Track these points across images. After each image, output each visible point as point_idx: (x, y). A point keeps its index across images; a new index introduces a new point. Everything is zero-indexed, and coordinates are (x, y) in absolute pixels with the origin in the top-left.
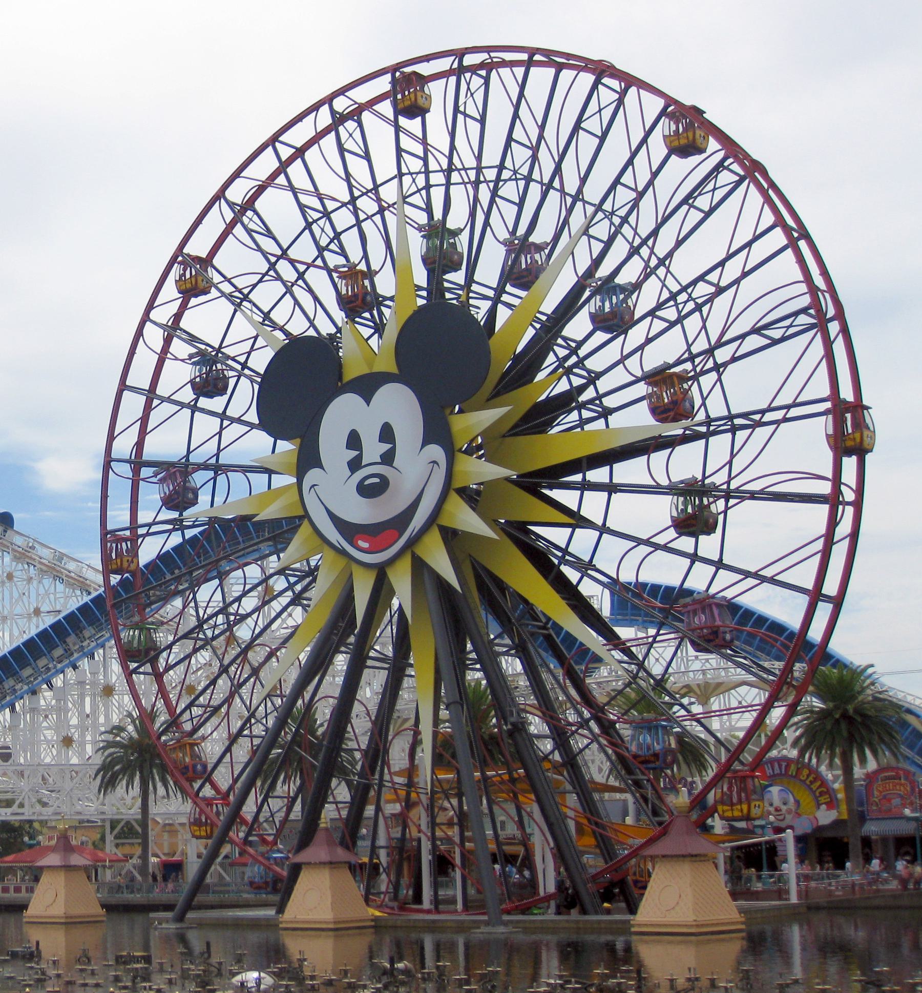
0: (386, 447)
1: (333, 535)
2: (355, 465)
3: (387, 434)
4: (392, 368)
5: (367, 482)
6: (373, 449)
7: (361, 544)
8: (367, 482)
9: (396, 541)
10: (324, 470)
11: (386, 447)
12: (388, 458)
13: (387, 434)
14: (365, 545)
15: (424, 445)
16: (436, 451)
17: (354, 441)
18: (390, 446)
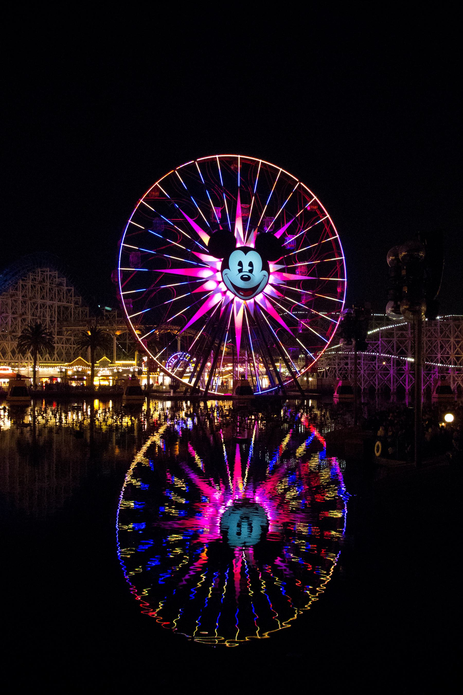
0: (251, 268)
1: (233, 289)
2: (240, 271)
3: (251, 264)
4: (252, 246)
5: (244, 277)
6: (246, 268)
7: (241, 293)
8: (244, 277)
9: (252, 295)
10: (229, 269)
11: (251, 268)
12: (251, 271)
13: (251, 264)
14: (242, 294)
15: (262, 270)
16: (265, 272)
18: (251, 268)
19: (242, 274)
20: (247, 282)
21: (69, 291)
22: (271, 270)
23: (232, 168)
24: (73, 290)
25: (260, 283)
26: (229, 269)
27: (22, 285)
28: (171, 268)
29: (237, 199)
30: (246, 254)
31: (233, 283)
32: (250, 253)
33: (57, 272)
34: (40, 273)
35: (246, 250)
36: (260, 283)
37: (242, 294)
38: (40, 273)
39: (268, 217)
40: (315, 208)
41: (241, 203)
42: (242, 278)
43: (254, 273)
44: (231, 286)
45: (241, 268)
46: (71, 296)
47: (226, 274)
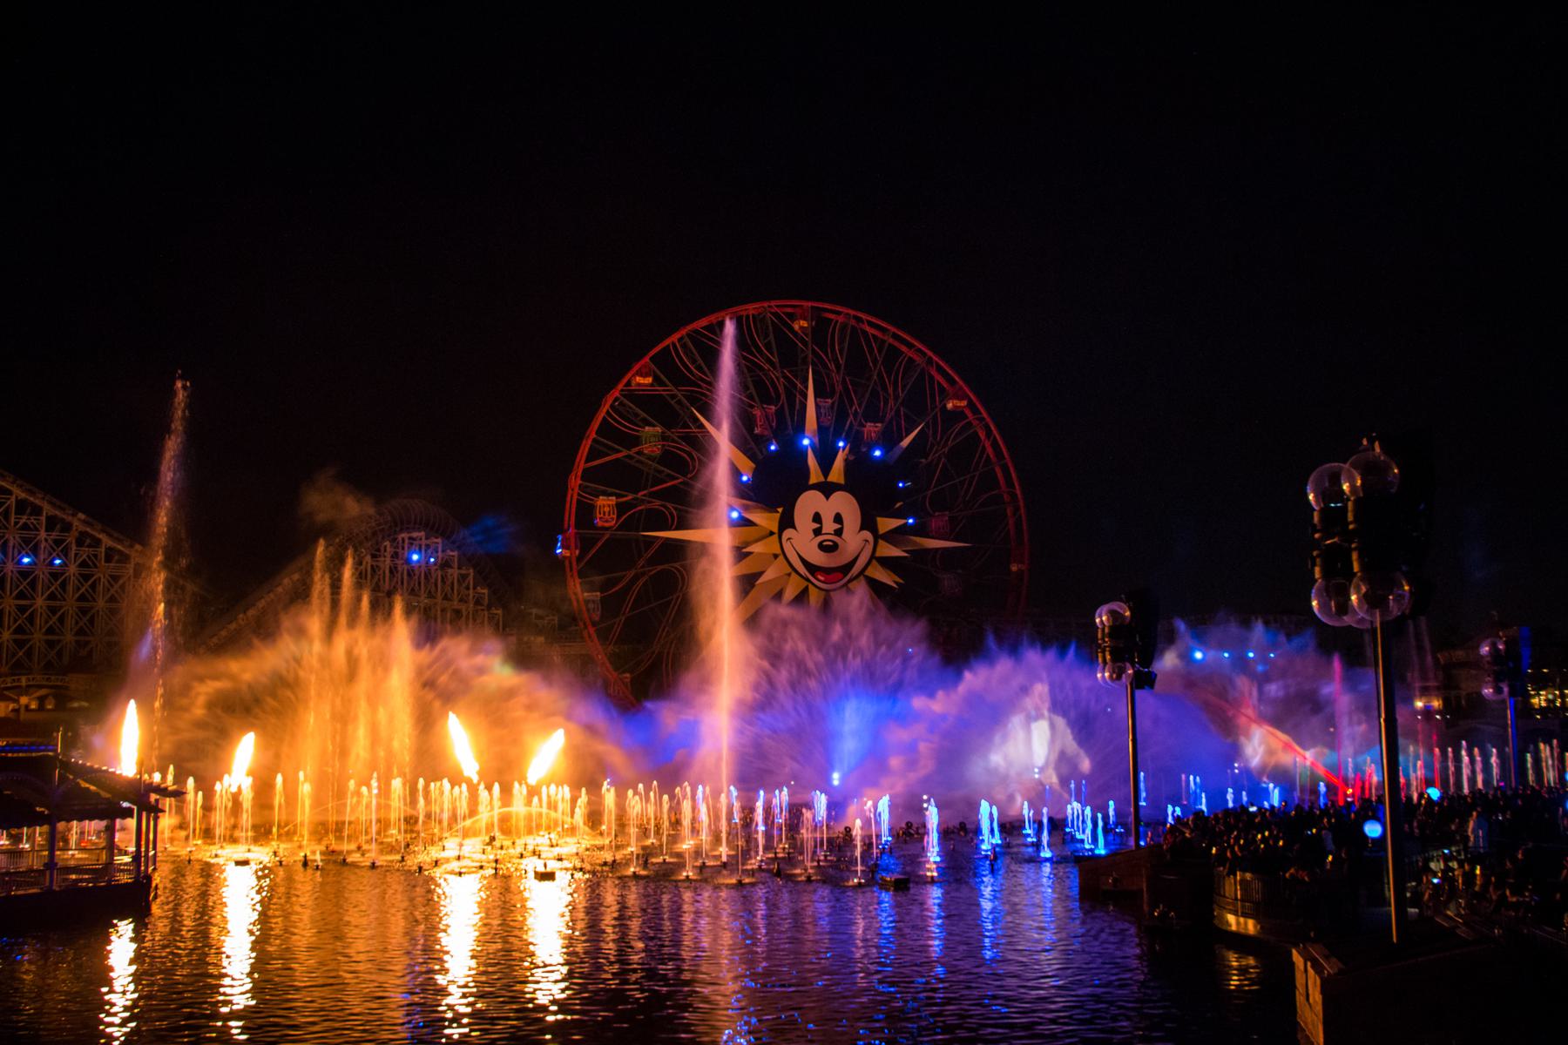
0: (840, 526)
2: (817, 532)
3: (838, 519)
4: (842, 481)
5: (825, 543)
6: (829, 526)
8: (825, 543)
12: (839, 532)
13: (838, 519)
14: (822, 578)
15: (862, 529)
16: (867, 535)
17: (817, 518)
19: (820, 538)
20: (832, 554)
21: (464, 577)
22: (882, 529)
23: (796, 327)
24: (471, 577)
26: (795, 528)
27: (372, 566)
28: (676, 529)
29: (807, 388)
30: (827, 499)
31: (806, 558)
33: (439, 540)
34: (407, 541)
35: (827, 489)
37: (822, 578)
38: (407, 541)
39: (869, 424)
41: (816, 397)
42: (821, 546)
43: (844, 536)
44: (801, 563)
45: (819, 525)
46: (468, 588)
47: (789, 539)
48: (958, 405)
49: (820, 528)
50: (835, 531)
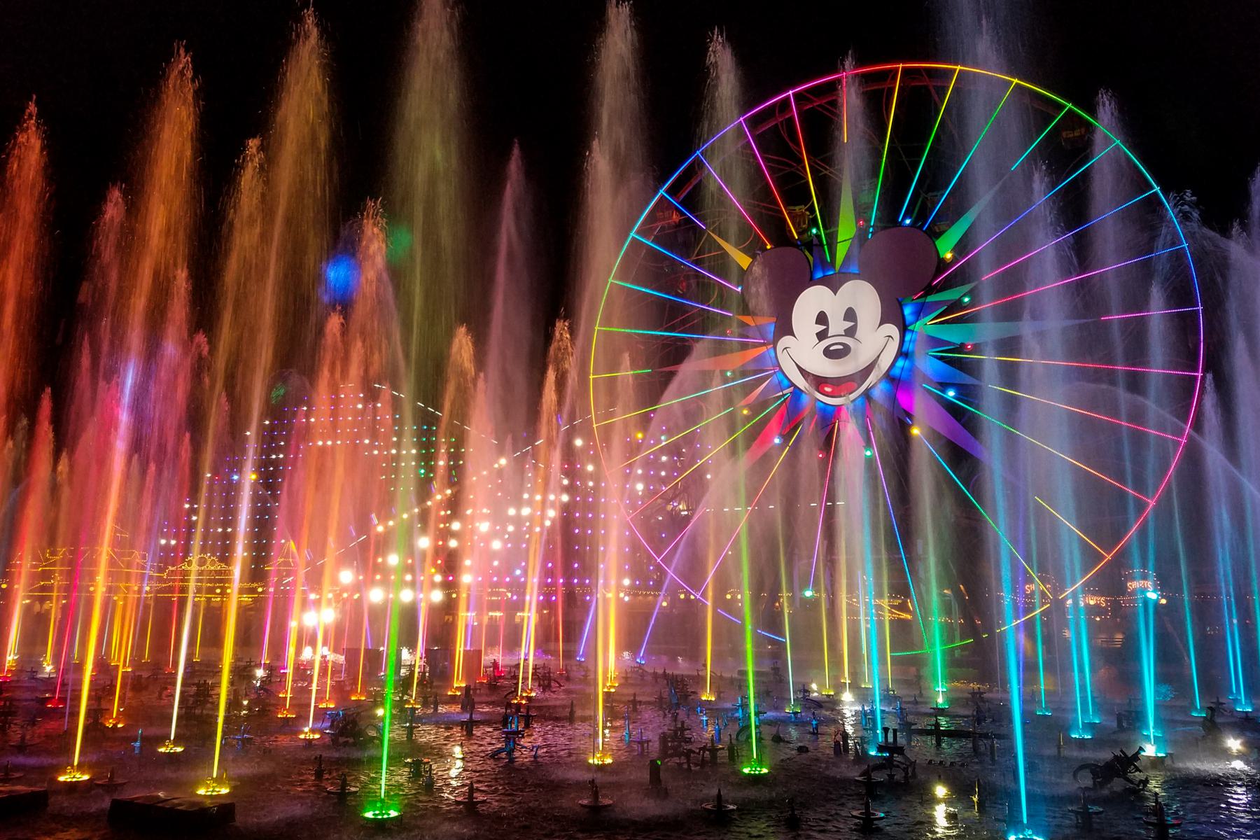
2: (822, 336)
3: (850, 315)
6: (837, 325)
8: (832, 348)
12: (851, 332)
13: (850, 315)
15: (881, 324)
16: (892, 330)
17: (822, 318)
19: (826, 343)
25: (879, 356)
32: (848, 287)
36: (879, 356)
40: (1077, 134)
42: (828, 353)
43: (858, 335)
45: (825, 327)
47: (786, 348)
48: (1071, 135)
49: (826, 331)
50: (845, 331)
